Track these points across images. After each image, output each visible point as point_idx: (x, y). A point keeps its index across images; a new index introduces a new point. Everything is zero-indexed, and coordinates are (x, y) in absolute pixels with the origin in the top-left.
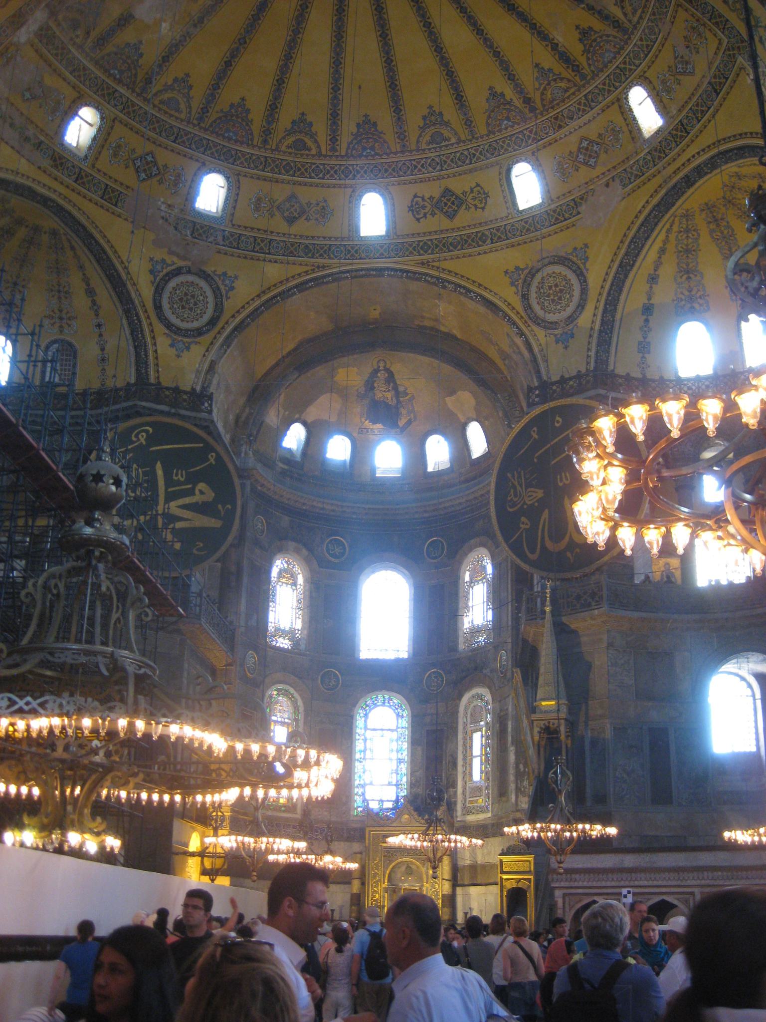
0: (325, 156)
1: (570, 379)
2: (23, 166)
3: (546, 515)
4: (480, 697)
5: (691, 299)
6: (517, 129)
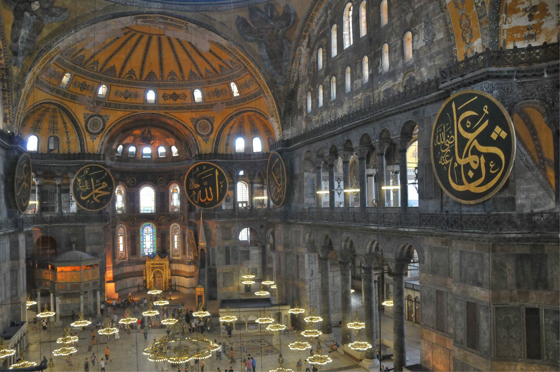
0: (138, 80)
1: (208, 154)
2: (48, 96)
3: (200, 192)
4: (176, 226)
5: (241, 133)
6: (197, 81)
